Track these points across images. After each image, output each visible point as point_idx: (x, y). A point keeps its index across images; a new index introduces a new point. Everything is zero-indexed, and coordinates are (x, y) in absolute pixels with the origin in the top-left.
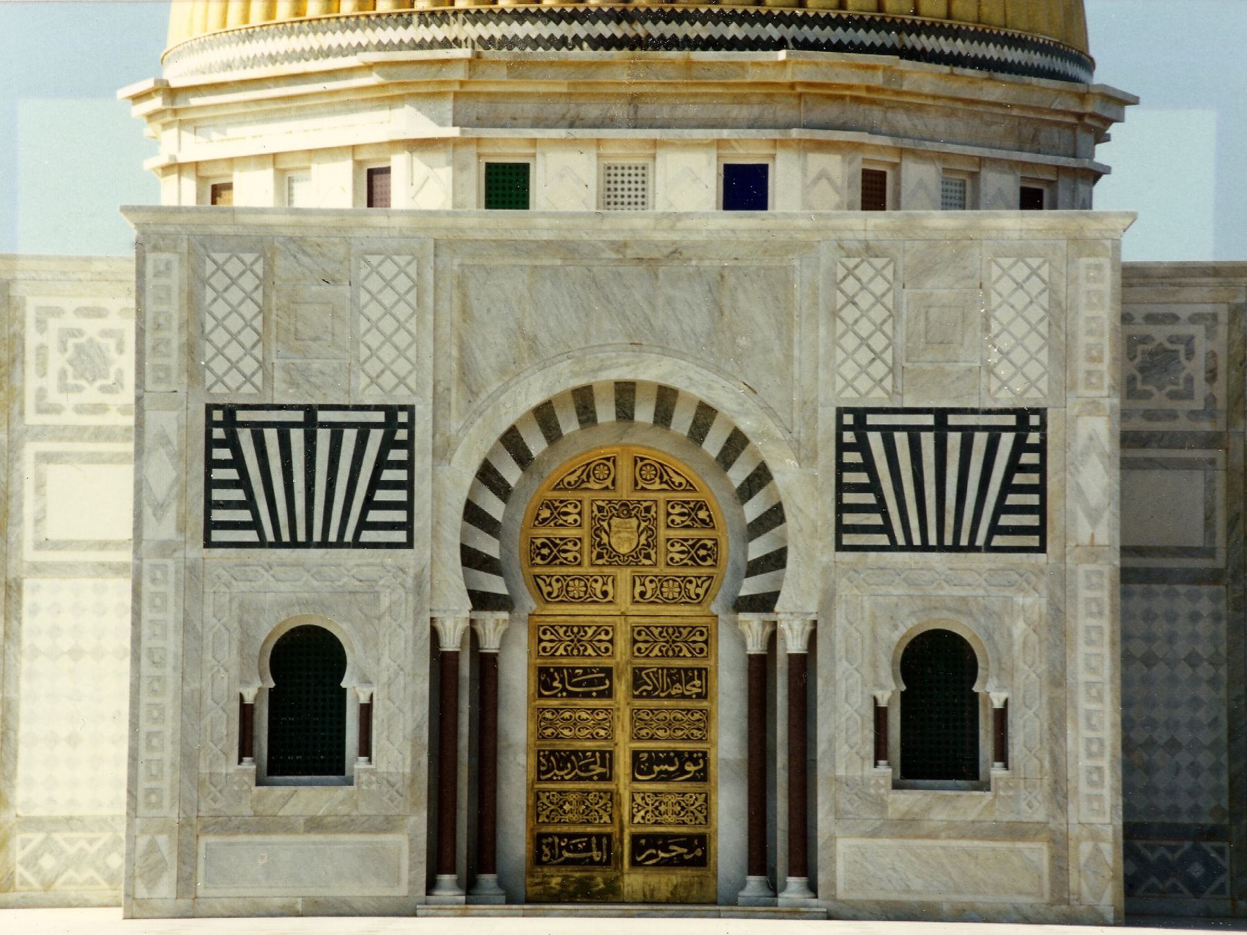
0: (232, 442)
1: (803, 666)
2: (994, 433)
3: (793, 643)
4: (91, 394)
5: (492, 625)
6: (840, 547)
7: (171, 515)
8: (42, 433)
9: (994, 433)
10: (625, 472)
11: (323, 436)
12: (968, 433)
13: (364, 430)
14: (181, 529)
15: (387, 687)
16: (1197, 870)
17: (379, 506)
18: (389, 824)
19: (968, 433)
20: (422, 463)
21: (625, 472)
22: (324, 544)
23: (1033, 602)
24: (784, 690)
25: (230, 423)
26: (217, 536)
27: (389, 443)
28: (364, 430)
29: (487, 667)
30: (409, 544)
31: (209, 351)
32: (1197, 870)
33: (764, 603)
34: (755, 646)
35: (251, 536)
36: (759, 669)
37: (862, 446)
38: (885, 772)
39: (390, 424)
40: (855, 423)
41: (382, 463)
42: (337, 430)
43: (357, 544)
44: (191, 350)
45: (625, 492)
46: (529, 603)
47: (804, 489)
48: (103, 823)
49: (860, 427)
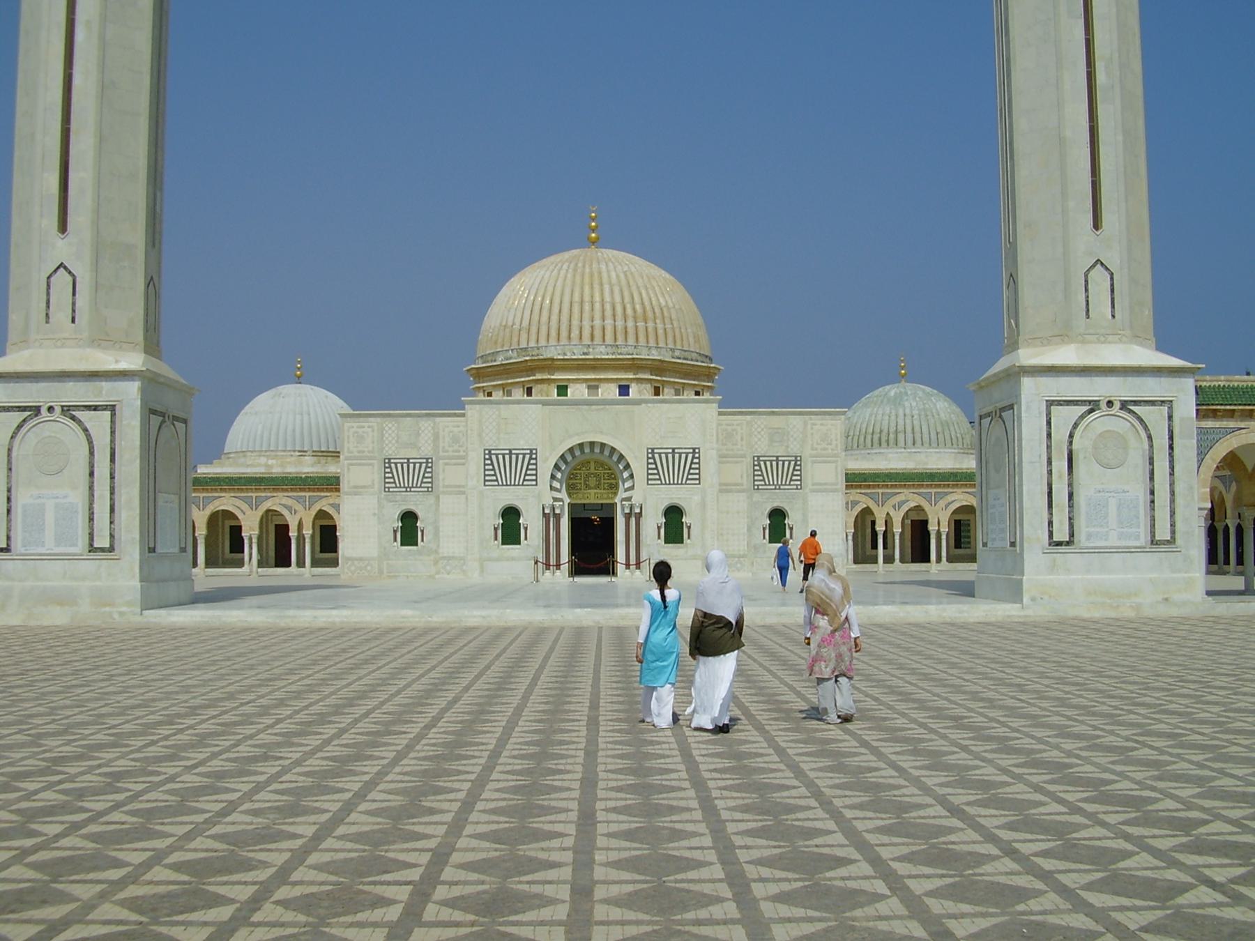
2: (687, 454)
3: (638, 510)
4: (456, 447)
5: (557, 504)
8: (444, 458)
9: (687, 454)
10: (592, 465)
12: (680, 454)
13: (524, 455)
15: (531, 521)
17: (530, 475)
19: (680, 454)
21: (592, 465)
23: (697, 498)
25: (490, 454)
27: (531, 458)
28: (524, 455)
33: (629, 499)
34: (627, 511)
37: (653, 458)
39: (531, 454)
41: (529, 464)
42: (517, 455)
44: (480, 435)
45: (592, 470)
46: (567, 500)
49: (653, 453)
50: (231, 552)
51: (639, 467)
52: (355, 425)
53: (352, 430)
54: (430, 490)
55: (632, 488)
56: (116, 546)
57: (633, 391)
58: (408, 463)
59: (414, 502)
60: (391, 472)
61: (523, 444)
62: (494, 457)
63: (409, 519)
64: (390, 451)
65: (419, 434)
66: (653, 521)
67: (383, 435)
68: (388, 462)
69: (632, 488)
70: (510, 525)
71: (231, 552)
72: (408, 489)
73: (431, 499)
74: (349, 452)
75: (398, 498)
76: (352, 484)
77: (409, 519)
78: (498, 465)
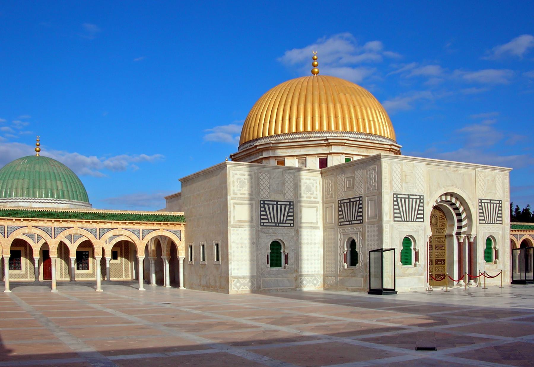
0: (397, 201)
6: (480, 223)
7: (388, 216)
11: (411, 200)
14: (390, 218)
16: (315, 282)
18: (421, 275)
20: (425, 206)
22: (411, 221)
26: (396, 219)
30: (423, 222)
31: (394, 183)
32: (315, 282)
35: (400, 219)
38: (269, 265)
39: (420, 199)
40: (481, 201)
43: (416, 221)
48: (244, 277)
50: (88, 269)
52: (239, 173)
53: (236, 177)
54: (292, 225)
58: (277, 204)
59: (281, 234)
60: (265, 211)
61: (415, 192)
62: (399, 200)
63: (276, 246)
64: (264, 195)
65: (284, 184)
67: (259, 183)
71: (88, 269)
72: (277, 224)
73: (292, 232)
74: (234, 193)
75: (271, 231)
76: (236, 219)
77: (276, 246)
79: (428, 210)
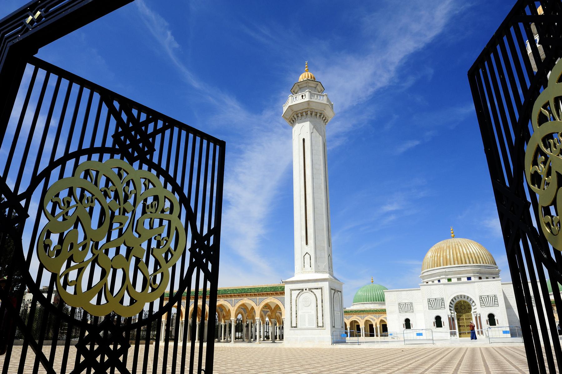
1: (480, 317)
15: (445, 320)
17: (442, 306)
24: (478, 318)
29: (453, 319)
33: (475, 312)
36: (476, 317)
47: (477, 301)
51: (477, 301)
54: (413, 312)
55: (476, 309)
56: (220, 138)
57: (473, 278)
63: (407, 322)
66: (485, 319)
68: (400, 304)
69: (476, 309)
70: (438, 322)
72: (406, 312)
77: (407, 322)
78: (432, 303)
79: (447, 304)
